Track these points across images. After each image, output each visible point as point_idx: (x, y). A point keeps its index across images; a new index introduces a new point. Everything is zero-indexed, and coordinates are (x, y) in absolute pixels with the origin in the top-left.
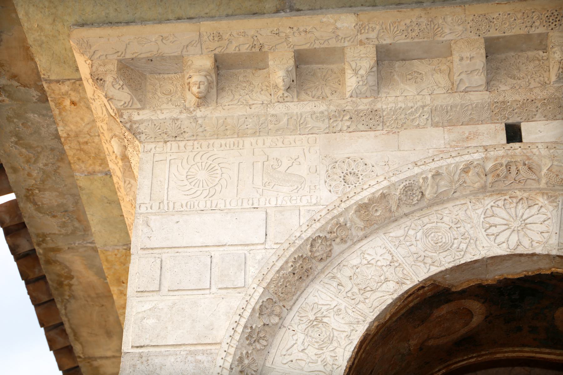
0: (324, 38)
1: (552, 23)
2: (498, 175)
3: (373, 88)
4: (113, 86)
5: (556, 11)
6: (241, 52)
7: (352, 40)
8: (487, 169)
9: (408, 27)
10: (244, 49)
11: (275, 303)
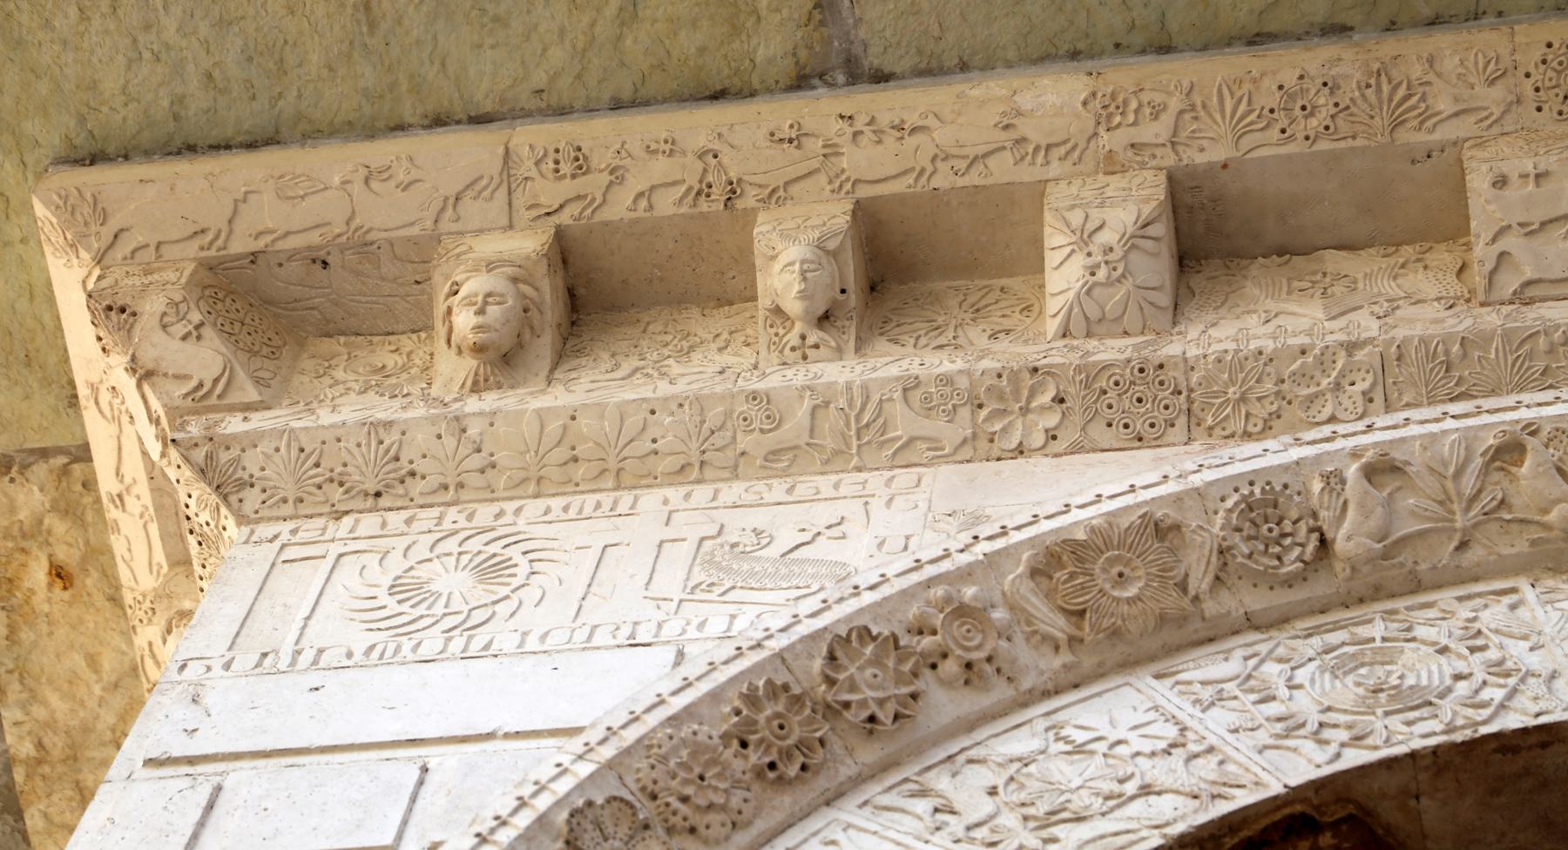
0: (964, 152)
4: (164, 327)
6: (656, 213)
7: (1076, 154)
9: (1292, 97)
10: (666, 204)
11: (646, 827)
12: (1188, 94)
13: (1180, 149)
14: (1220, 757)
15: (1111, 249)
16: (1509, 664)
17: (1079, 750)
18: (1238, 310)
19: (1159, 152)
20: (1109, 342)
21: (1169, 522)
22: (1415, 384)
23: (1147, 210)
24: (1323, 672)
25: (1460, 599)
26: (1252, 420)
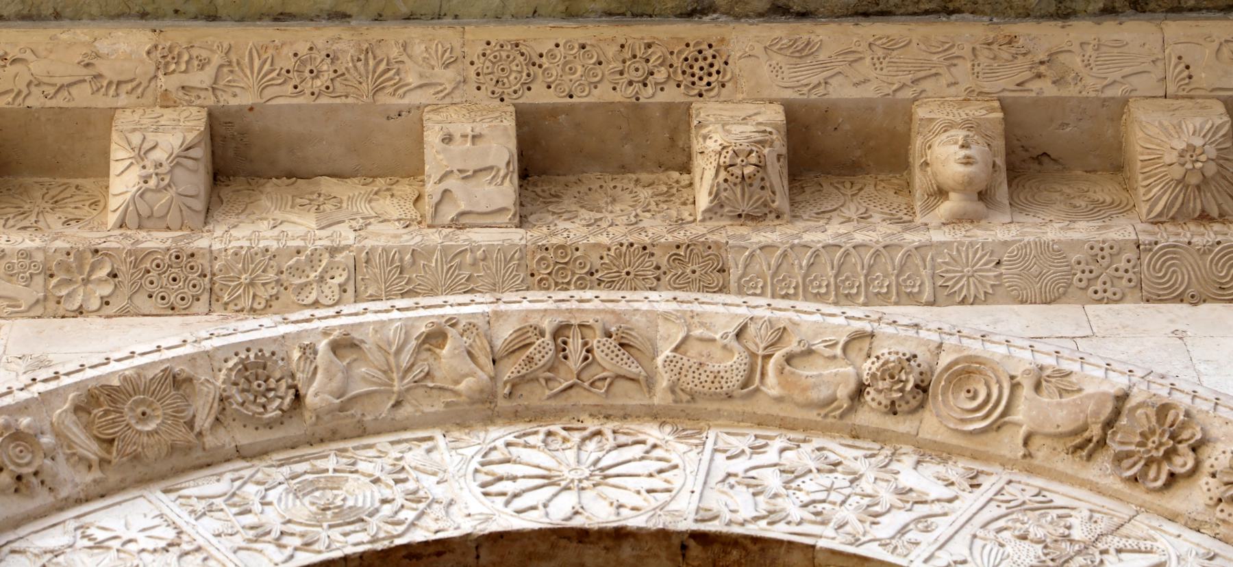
0: (54, 80)
1: (701, 79)
2: (530, 359)
3: (190, 201)
5: (710, 46)
8: (499, 343)
9: (303, 63)
12: (227, 53)
13: (219, 93)
14: (205, 555)
15: (161, 165)
16: (421, 494)
17: (99, 545)
18: (254, 217)
19: (202, 94)
20: (155, 234)
21: (184, 375)
22: (377, 281)
23: (190, 137)
24: (288, 493)
25: (392, 443)
26: (258, 300)
